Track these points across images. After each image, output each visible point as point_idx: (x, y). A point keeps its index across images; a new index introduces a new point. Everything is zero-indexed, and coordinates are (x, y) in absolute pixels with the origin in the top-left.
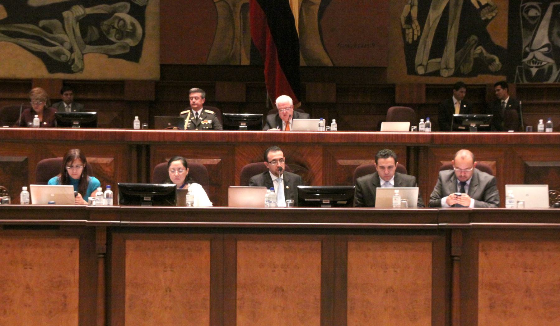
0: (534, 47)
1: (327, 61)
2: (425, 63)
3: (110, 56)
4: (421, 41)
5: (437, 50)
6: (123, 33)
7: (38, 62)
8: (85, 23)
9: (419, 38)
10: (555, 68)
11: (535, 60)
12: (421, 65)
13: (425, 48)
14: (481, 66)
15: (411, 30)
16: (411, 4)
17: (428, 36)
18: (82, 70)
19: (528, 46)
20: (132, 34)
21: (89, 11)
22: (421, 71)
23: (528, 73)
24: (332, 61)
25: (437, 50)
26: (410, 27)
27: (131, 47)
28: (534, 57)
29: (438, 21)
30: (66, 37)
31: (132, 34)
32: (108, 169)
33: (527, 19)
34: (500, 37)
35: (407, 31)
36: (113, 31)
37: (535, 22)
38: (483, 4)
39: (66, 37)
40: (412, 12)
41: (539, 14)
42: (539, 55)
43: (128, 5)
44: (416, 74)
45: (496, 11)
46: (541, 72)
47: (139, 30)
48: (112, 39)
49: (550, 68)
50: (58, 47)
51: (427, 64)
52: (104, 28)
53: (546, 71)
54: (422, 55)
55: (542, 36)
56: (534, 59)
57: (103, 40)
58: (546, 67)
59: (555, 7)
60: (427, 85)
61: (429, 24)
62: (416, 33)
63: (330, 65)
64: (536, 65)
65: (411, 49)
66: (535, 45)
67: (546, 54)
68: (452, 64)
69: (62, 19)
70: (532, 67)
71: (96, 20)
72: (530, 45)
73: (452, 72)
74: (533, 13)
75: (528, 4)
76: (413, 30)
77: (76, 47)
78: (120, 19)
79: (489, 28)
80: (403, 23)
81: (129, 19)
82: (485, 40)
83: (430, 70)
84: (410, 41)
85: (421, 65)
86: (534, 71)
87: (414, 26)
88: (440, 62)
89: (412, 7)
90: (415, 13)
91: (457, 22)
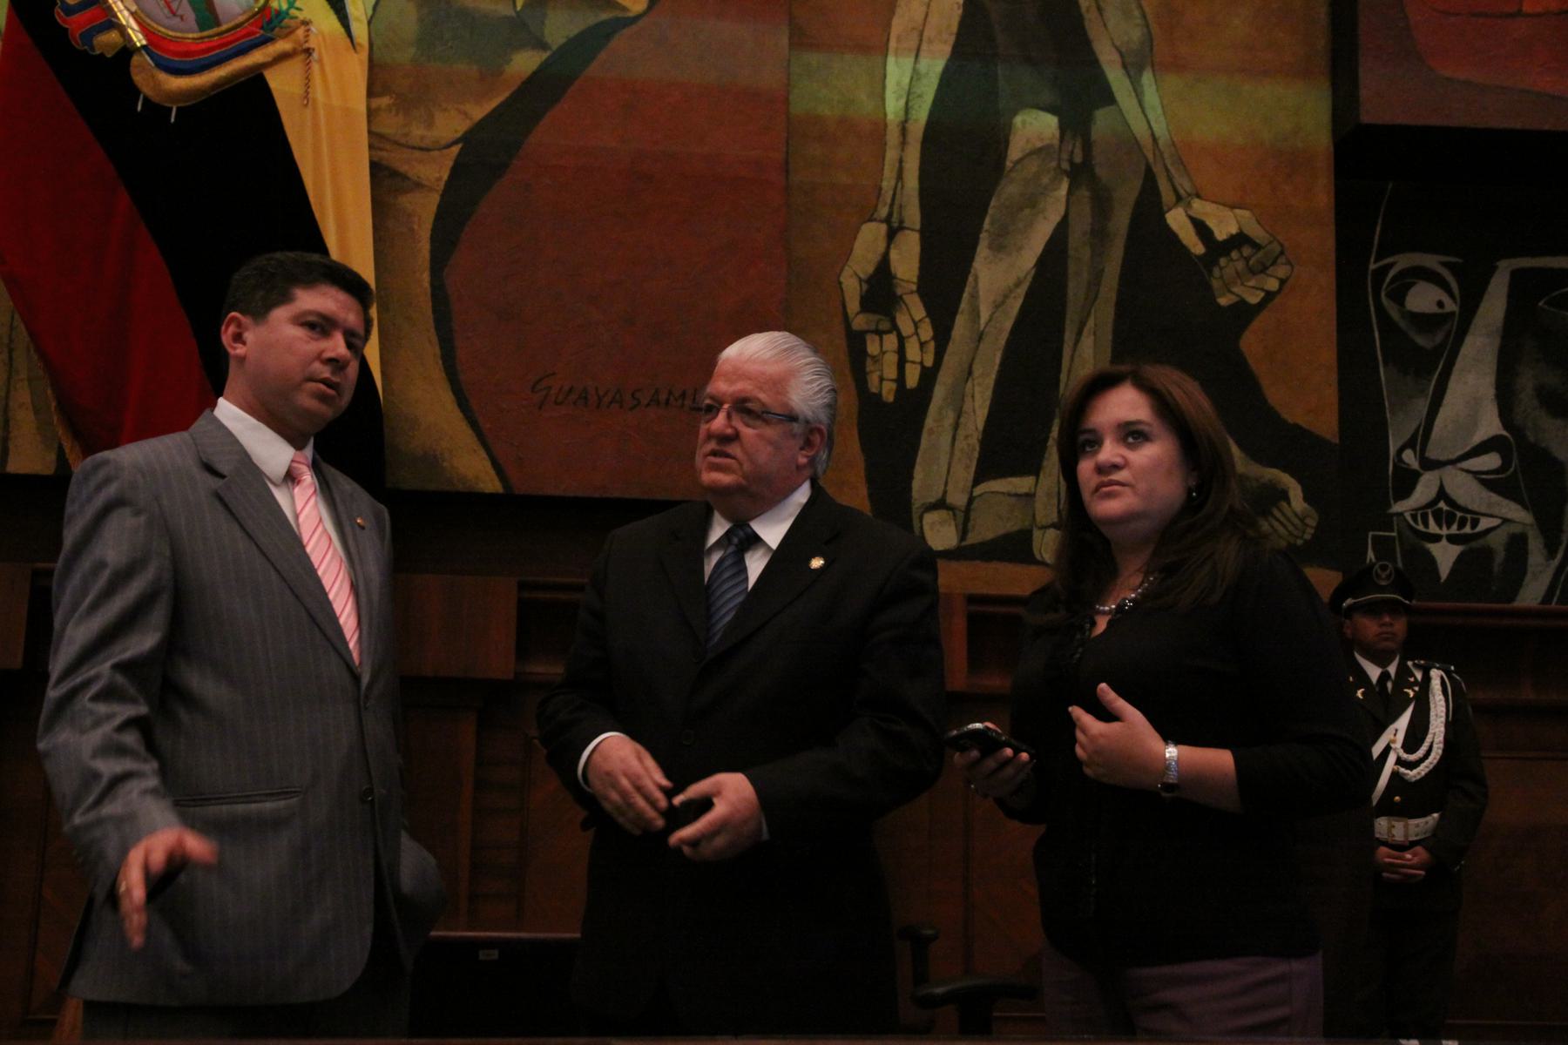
0: (1433, 453)
2: (958, 499)
4: (939, 392)
9: (929, 376)
10: (1535, 545)
11: (1446, 508)
12: (941, 504)
13: (956, 426)
15: (891, 341)
16: (888, 220)
17: (970, 373)
19: (1410, 444)
24: (495, 464)
26: (885, 325)
28: (1442, 494)
29: (1015, 305)
33: (1403, 324)
35: (872, 347)
37: (1439, 338)
38: (1221, 234)
40: (894, 255)
41: (1451, 306)
45: (1282, 271)
46: (1475, 558)
49: (1518, 544)
51: (971, 500)
53: (1500, 556)
54: (944, 459)
55: (1470, 402)
56: (1442, 505)
58: (1497, 541)
59: (1517, 276)
60: (972, 599)
61: (975, 313)
62: (913, 352)
63: (491, 484)
64: (1454, 529)
66: (1443, 440)
70: (1436, 538)
72: (1421, 438)
74: (1423, 298)
75: (1403, 261)
76: (902, 340)
79: (1251, 343)
80: (853, 305)
83: (986, 529)
84: (888, 392)
85: (941, 504)
86: (1445, 556)
87: (906, 327)
88: (1030, 496)
89: (891, 235)
90: (906, 263)
91: (1104, 313)
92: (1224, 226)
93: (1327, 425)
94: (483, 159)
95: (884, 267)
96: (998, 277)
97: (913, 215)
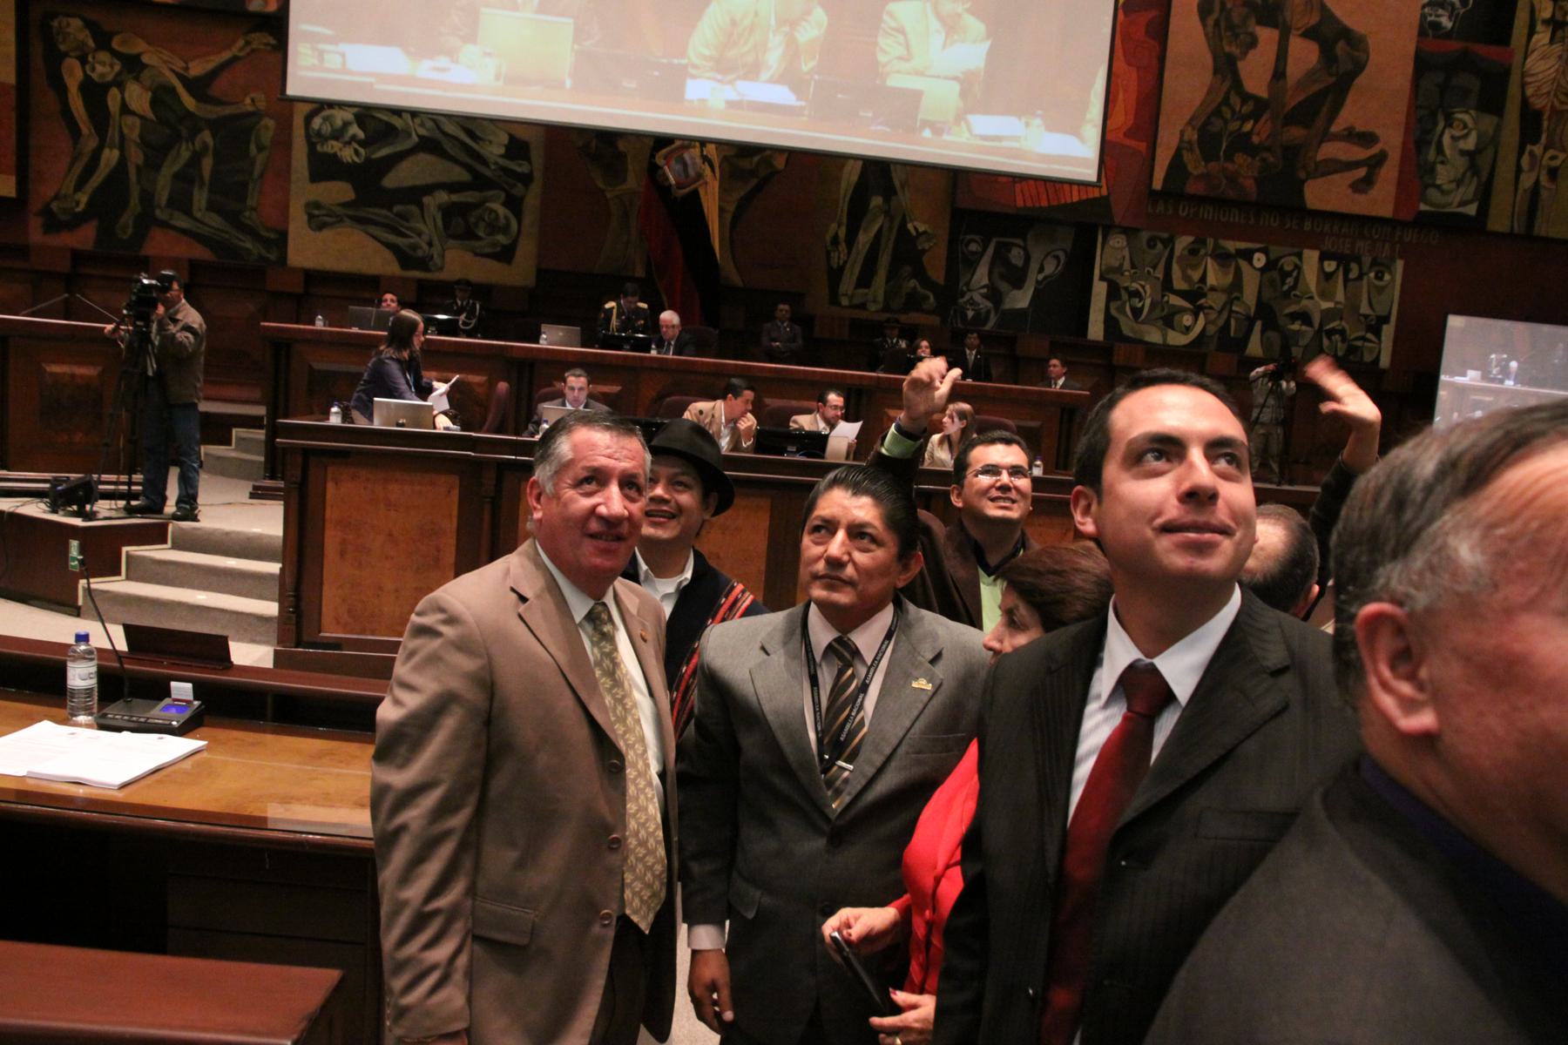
1: (737, 280)
3: (476, 254)
5: (865, 280)
6: (493, 228)
7: (388, 255)
8: (448, 212)
11: (972, 302)
14: (913, 303)
18: (441, 269)
20: (505, 230)
21: (455, 198)
22: (845, 302)
23: (964, 315)
25: (865, 280)
27: (504, 246)
30: (426, 229)
31: (505, 230)
32: (479, 390)
34: (937, 273)
36: (482, 225)
39: (426, 229)
42: (977, 297)
43: (503, 195)
44: (839, 304)
47: (514, 225)
48: (481, 234)
49: (988, 312)
50: (415, 240)
52: (472, 220)
54: (847, 284)
55: (981, 276)
57: (469, 235)
65: (835, 275)
67: (985, 296)
68: (881, 298)
69: (421, 206)
71: (462, 210)
72: (968, 284)
73: (880, 306)
74: (973, 247)
75: (969, 237)
77: (436, 242)
78: (491, 211)
79: (925, 259)
81: (502, 211)
82: (920, 273)
83: (856, 301)
86: (970, 314)
90: (842, 233)
92: (921, 229)
93: (941, 281)
94: (744, 204)
95: (836, 236)
96: (864, 238)
97: (845, 221)
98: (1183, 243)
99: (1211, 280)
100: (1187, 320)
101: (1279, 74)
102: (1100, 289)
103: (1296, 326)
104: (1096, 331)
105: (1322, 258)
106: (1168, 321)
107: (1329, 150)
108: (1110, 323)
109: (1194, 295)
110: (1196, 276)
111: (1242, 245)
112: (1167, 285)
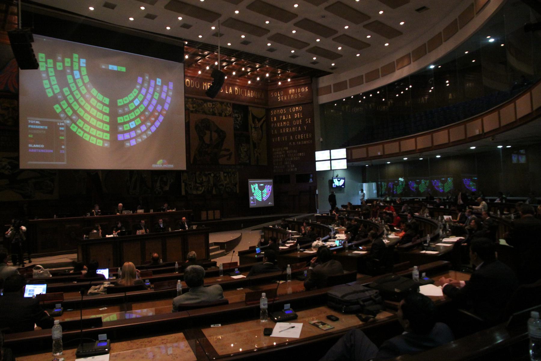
55: (158, 184)
74: (156, 178)
98: (198, 173)
99: (204, 180)
100: (201, 188)
101: (211, 139)
102: (183, 184)
103: (221, 187)
104: (183, 193)
105: (224, 173)
106: (197, 189)
107: (223, 153)
108: (186, 191)
109: (201, 183)
110: (201, 179)
111: (209, 172)
112: (196, 182)
